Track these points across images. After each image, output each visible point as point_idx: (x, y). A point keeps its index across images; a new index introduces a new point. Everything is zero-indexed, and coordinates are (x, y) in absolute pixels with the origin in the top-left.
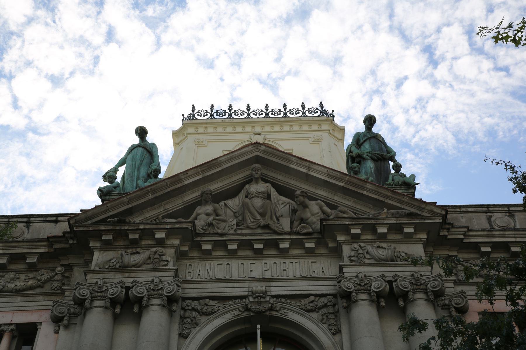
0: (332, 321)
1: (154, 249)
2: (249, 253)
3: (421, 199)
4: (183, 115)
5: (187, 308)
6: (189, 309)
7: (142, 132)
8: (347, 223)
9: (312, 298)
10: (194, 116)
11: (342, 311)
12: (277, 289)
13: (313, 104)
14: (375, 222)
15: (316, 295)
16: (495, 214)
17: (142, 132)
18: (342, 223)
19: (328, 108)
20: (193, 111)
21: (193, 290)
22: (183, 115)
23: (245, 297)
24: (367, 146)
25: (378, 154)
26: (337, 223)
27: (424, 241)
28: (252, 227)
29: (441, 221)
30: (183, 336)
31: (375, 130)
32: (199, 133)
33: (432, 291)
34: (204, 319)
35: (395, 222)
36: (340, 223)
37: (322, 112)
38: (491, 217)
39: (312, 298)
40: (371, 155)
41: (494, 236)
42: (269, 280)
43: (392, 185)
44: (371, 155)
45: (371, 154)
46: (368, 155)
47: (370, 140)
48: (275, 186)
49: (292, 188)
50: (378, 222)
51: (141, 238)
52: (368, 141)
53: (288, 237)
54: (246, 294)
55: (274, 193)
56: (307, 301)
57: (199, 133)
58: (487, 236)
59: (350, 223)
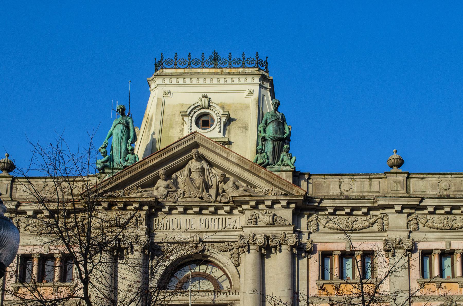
3: (300, 172)
4: (156, 59)
5: (155, 249)
6: (156, 250)
8: (247, 199)
14: (264, 199)
15: (229, 242)
16: (345, 180)
18: (244, 199)
22: (156, 59)
23: (188, 243)
25: (276, 137)
26: (241, 199)
27: (293, 209)
28: (192, 197)
29: (302, 198)
32: (166, 85)
33: (290, 245)
35: (276, 199)
36: (243, 199)
38: (342, 182)
39: (226, 243)
40: (271, 138)
41: (335, 203)
42: (202, 232)
43: (281, 165)
44: (271, 138)
45: (272, 137)
46: (269, 138)
47: (273, 123)
49: (218, 164)
50: (265, 199)
52: (272, 123)
53: (214, 204)
54: (189, 240)
56: (222, 245)
57: (166, 85)
58: (332, 203)
59: (249, 199)
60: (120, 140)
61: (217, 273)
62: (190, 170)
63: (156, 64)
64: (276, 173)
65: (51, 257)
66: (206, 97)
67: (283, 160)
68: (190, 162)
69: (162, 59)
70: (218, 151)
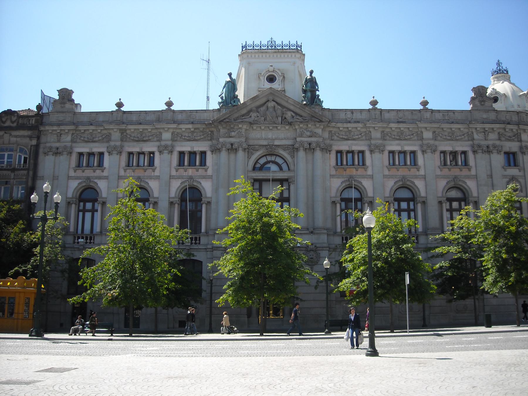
0: (292, 155)
1: (239, 130)
2: (268, 129)
7: (230, 75)
9: (287, 146)
10: (246, 47)
11: (295, 153)
12: (277, 143)
13: (293, 42)
17: (230, 75)
19: (299, 43)
20: (246, 44)
21: (251, 142)
24: (309, 84)
30: (249, 158)
31: (313, 75)
34: (254, 152)
37: (297, 46)
48: (277, 103)
51: (234, 126)
55: (276, 105)
60: (230, 91)
61: (279, 161)
62: (267, 107)
63: (242, 47)
64: (313, 109)
65: (195, 153)
66: (272, 66)
67: (316, 102)
68: (267, 103)
69: (246, 44)
70: (283, 98)
